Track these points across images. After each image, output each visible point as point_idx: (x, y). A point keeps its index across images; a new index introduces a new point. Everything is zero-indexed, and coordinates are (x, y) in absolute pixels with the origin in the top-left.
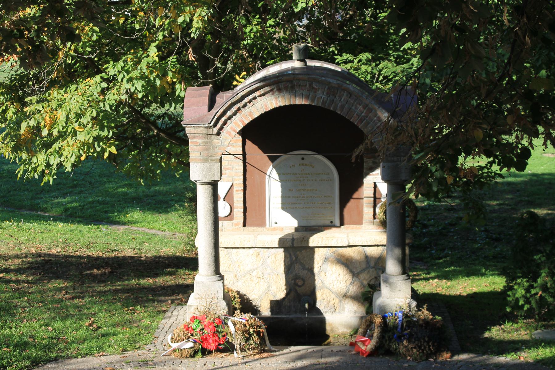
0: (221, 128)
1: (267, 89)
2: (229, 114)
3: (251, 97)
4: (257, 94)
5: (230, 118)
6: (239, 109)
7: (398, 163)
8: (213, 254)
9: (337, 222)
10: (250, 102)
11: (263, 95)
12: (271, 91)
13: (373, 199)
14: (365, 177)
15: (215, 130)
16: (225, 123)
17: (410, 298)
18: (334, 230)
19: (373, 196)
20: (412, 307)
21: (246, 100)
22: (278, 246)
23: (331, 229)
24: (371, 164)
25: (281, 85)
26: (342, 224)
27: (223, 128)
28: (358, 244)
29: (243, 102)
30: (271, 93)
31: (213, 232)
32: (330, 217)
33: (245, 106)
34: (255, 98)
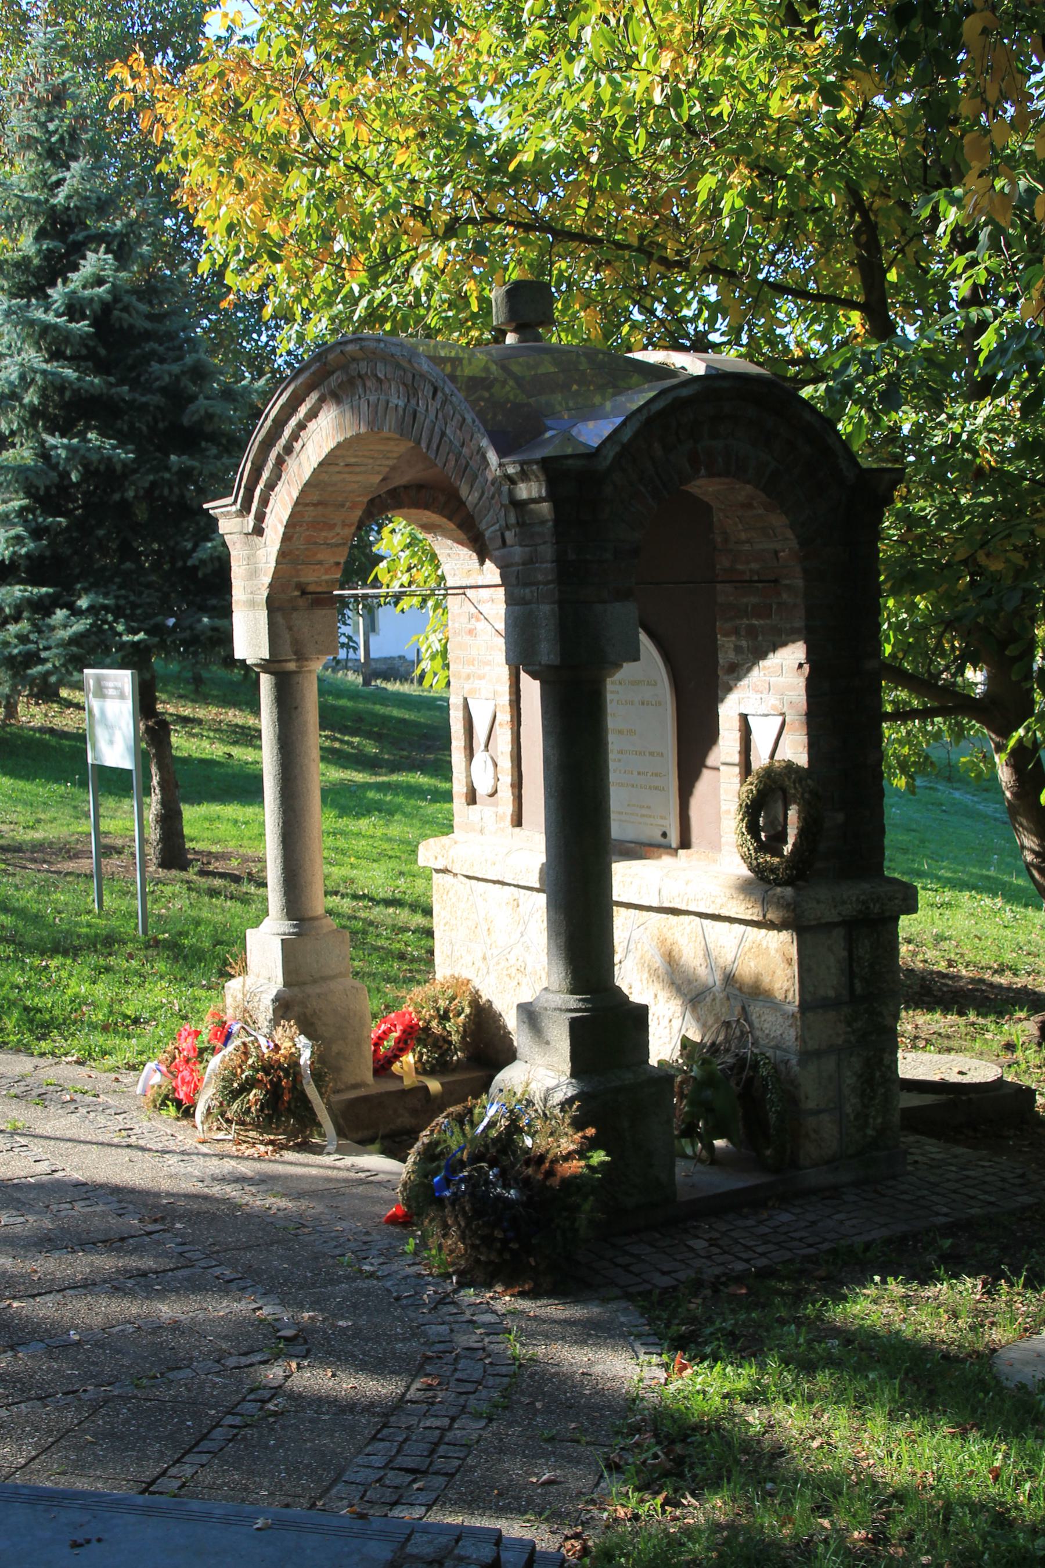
0: (260, 517)
1: (314, 397)
2: (265, 475)
3: (293, 422)
4: (303, 410)
5: (271, 486)
6: (280, 462)
7: (534, 606)
8: (279, 861)
9: (674, 839)
10: (295, 437)
11: (313, 414)
12: (322, 400)
13: (737, 770)
14: (722, 701)
15: (250, 521)
16: (265, 502)
17: (568, 1074)
18: (667, 860)
19: (736, 758)
20: (550, 1103)
21: (287, 432)
22: (537, 885)
23: (659, 857)
24: (732, 656)
25: (334, 380)
26: (685, 843)
27: (265, 514)
28: (684, 907)
29: (282, 441)
30: (325, 408)
31: (278, 801)
32: (662, 818)
33: (288, 449)
34: (302, 426)
